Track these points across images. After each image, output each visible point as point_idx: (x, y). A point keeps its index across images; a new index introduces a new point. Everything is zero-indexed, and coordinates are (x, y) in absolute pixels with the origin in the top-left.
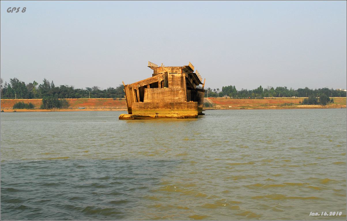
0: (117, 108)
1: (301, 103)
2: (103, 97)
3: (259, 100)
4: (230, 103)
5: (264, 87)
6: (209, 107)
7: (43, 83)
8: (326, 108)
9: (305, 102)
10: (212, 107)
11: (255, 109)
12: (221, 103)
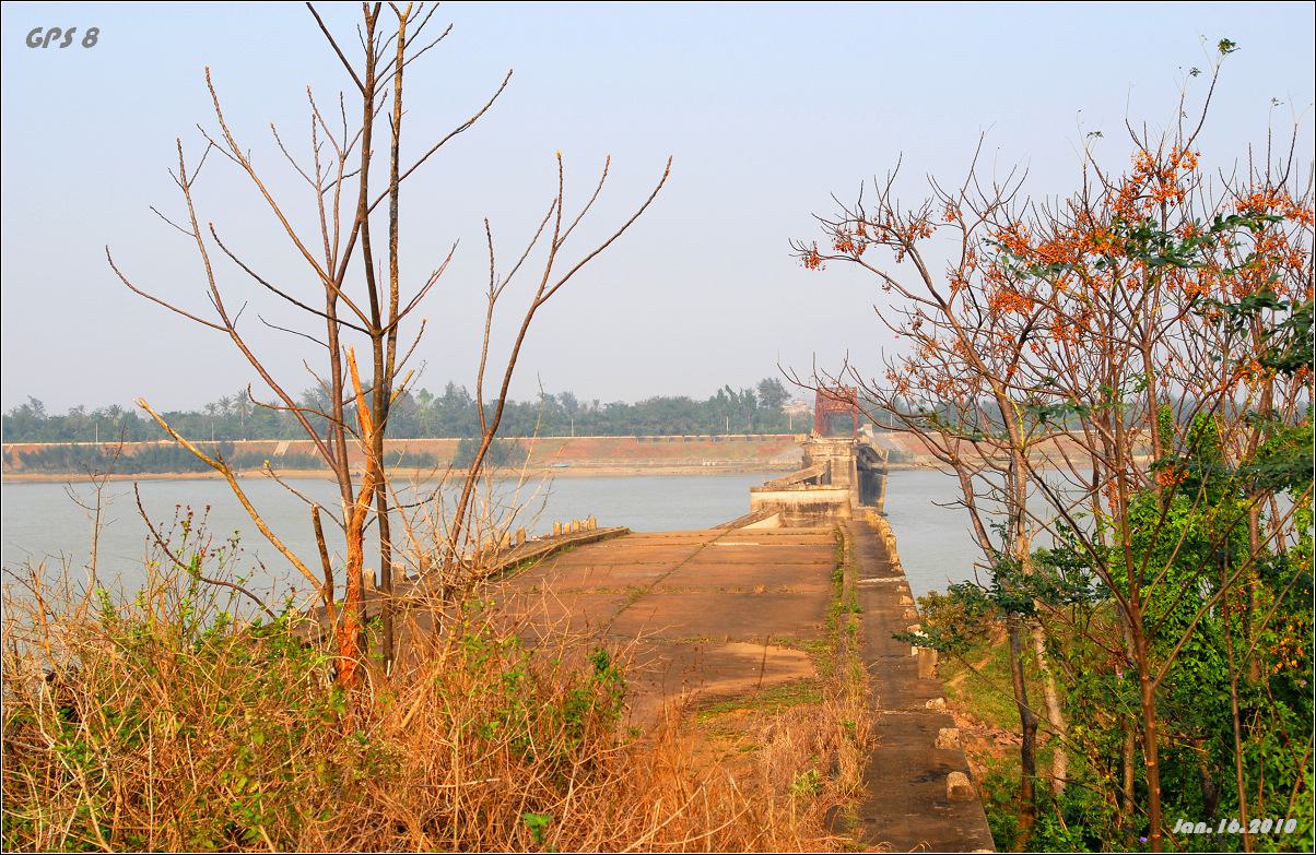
0: (652, 463)
2: (611, 432)
6: (897, 463)
7: (445, 394)
10: (903, 462)
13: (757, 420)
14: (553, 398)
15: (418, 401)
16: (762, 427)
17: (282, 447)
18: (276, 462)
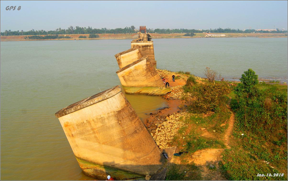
1: (183, 36)
3: (169, 34)
4: (157, 35)
5: (170, 29)
8: (192, 38)
9: (185, 35)
11: (166, 38)
12: (154, 35)
13: (131, 32)
14: (103, 29)
15: (84, 29)
16: (131, 32)
17: (65, 35)
18: (64, 37)
